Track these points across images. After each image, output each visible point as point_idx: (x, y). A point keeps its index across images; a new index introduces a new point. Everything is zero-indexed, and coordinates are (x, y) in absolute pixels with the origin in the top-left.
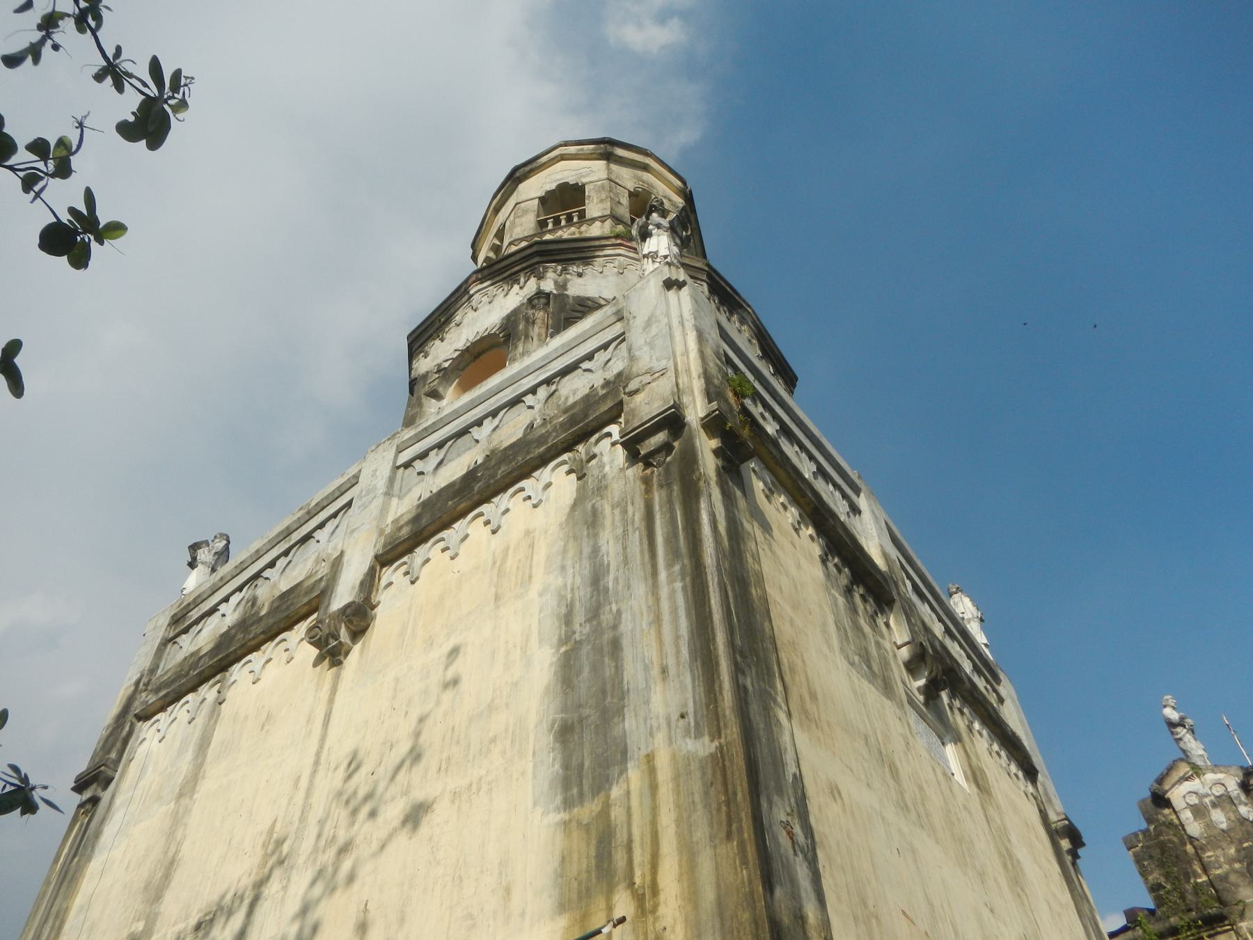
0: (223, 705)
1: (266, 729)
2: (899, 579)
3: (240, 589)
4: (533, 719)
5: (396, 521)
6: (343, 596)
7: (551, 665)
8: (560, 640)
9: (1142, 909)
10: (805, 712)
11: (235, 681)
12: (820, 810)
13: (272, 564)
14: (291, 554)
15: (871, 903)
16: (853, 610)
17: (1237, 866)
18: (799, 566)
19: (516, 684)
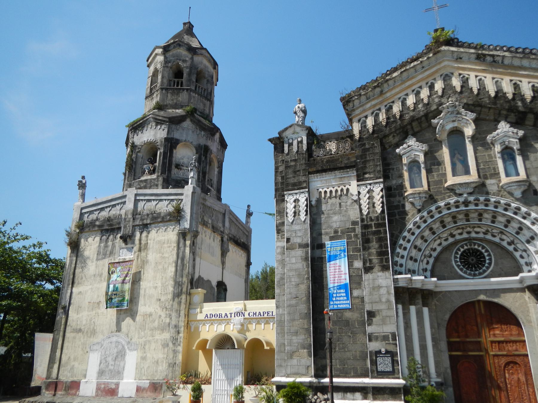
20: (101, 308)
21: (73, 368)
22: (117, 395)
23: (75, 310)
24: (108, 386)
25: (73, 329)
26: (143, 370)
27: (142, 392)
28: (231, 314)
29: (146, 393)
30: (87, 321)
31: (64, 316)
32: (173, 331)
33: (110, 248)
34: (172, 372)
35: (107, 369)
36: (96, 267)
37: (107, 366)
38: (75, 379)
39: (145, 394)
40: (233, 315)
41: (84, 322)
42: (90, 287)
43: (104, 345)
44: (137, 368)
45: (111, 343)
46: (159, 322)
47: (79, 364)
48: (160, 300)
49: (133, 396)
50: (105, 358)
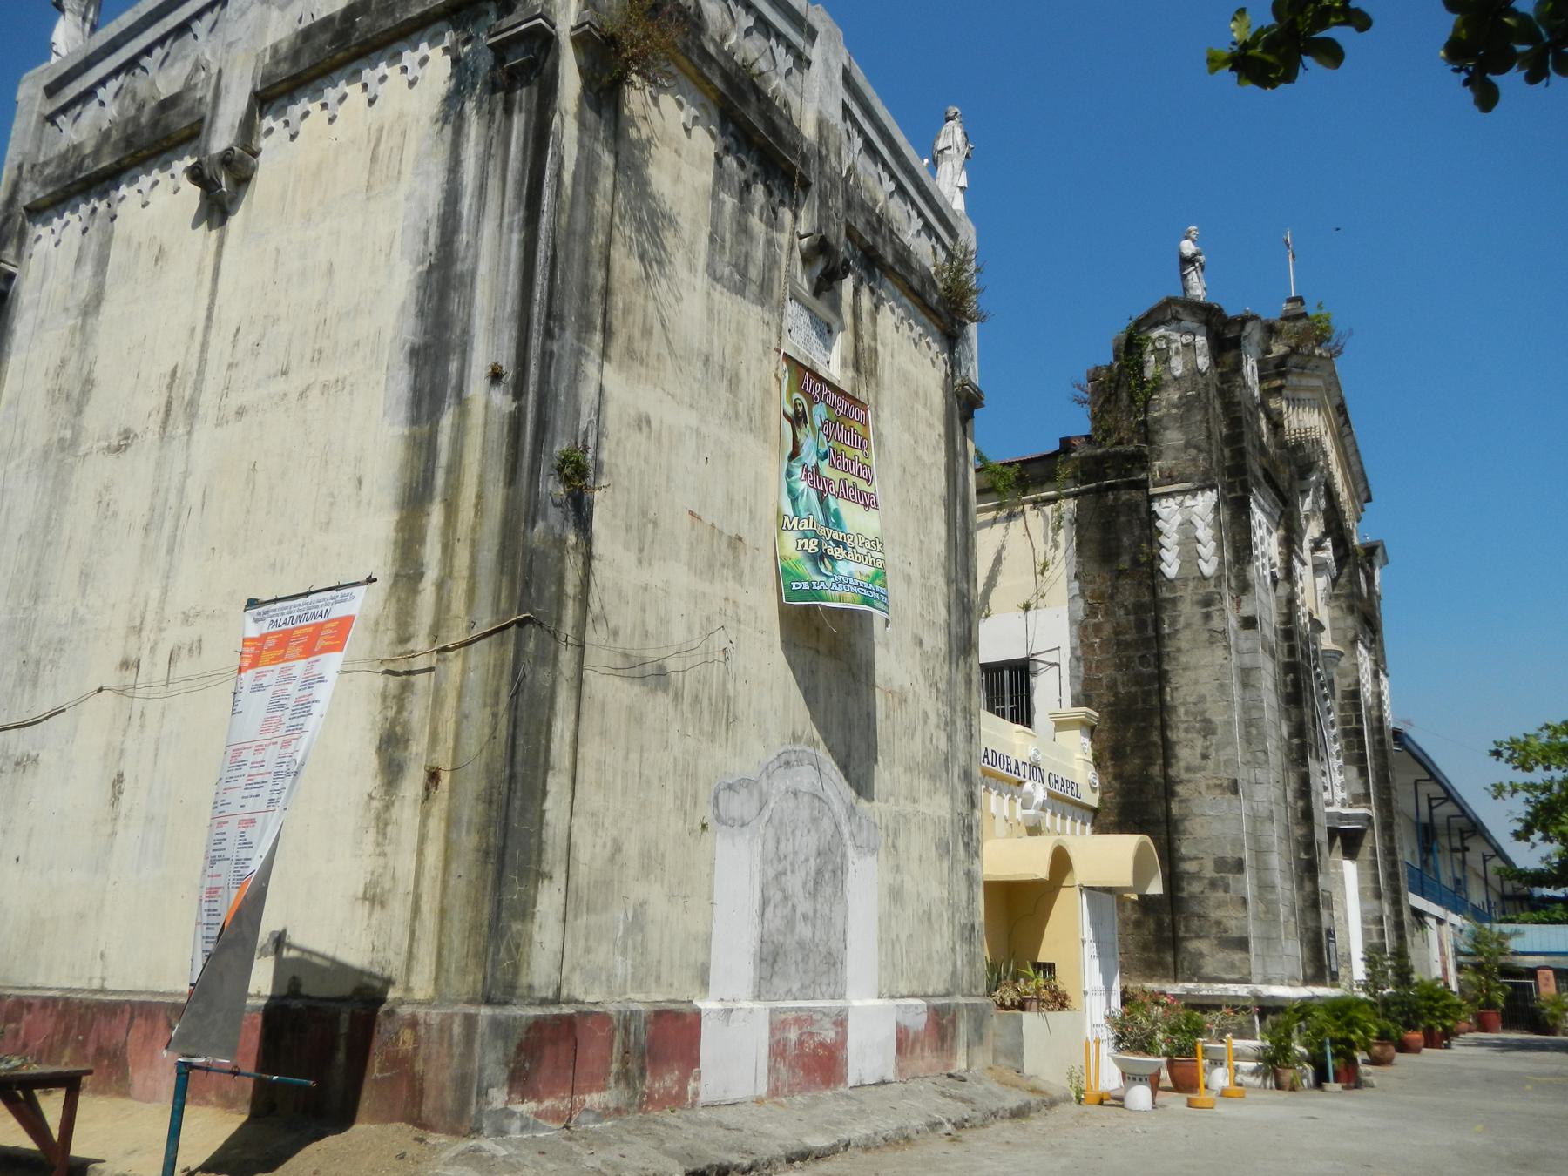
0: (116, 222)
1: (160, 263)
2: (832, 149)
3: (115, 73)
4: (388, 336)
5: (275, 49)
6: (221, 139)
7: (409, 281)
8: (418, 257)
9: (1079, 437)
10: (630, 353)
11: (123, 198)
12: (618, 443)
13: (148, 51)
14: (168, 42)
15: (651, 514)
16: (744, 208)
17: (1174, 411)
18: (677, 178)
19: (378, 292)
20: (747, 578)
21: (637, 923)
22: (843, 1078)
23: (628, 528)
24: (811, 1034)
25: (626, 656)
26: (897, 948)
27: (912, 1052)
28: (1024, 763)
29: (923, 1058)
30: (690, 630)
31: (572, 538)
32: (961, 792)
33: (759, 253)
34: (969, 963)
35: (791, 942)
36: (710, 312)
37: (790, 923)
38: (659, 996)
39: (920, 1063)
40: (1027, 768)
41: (678, 634)
42: (691, 419)
43: (771, 805)
44: (881, 941)
45: (795, 794)
46: (923, 741)
47: (671, 897)
48: (921, 643)
49: (890, 1076)
50: (780, 875)
